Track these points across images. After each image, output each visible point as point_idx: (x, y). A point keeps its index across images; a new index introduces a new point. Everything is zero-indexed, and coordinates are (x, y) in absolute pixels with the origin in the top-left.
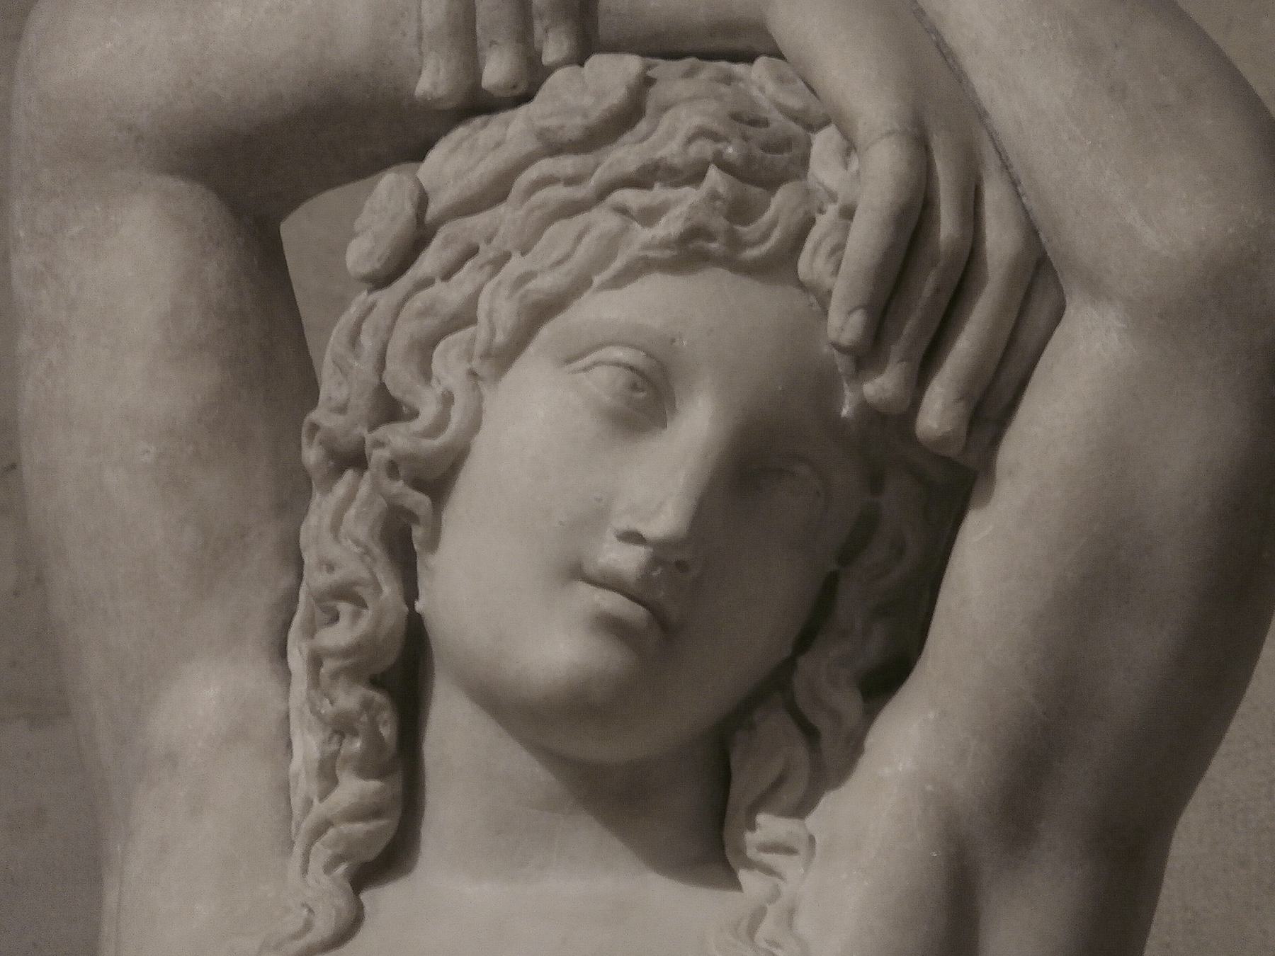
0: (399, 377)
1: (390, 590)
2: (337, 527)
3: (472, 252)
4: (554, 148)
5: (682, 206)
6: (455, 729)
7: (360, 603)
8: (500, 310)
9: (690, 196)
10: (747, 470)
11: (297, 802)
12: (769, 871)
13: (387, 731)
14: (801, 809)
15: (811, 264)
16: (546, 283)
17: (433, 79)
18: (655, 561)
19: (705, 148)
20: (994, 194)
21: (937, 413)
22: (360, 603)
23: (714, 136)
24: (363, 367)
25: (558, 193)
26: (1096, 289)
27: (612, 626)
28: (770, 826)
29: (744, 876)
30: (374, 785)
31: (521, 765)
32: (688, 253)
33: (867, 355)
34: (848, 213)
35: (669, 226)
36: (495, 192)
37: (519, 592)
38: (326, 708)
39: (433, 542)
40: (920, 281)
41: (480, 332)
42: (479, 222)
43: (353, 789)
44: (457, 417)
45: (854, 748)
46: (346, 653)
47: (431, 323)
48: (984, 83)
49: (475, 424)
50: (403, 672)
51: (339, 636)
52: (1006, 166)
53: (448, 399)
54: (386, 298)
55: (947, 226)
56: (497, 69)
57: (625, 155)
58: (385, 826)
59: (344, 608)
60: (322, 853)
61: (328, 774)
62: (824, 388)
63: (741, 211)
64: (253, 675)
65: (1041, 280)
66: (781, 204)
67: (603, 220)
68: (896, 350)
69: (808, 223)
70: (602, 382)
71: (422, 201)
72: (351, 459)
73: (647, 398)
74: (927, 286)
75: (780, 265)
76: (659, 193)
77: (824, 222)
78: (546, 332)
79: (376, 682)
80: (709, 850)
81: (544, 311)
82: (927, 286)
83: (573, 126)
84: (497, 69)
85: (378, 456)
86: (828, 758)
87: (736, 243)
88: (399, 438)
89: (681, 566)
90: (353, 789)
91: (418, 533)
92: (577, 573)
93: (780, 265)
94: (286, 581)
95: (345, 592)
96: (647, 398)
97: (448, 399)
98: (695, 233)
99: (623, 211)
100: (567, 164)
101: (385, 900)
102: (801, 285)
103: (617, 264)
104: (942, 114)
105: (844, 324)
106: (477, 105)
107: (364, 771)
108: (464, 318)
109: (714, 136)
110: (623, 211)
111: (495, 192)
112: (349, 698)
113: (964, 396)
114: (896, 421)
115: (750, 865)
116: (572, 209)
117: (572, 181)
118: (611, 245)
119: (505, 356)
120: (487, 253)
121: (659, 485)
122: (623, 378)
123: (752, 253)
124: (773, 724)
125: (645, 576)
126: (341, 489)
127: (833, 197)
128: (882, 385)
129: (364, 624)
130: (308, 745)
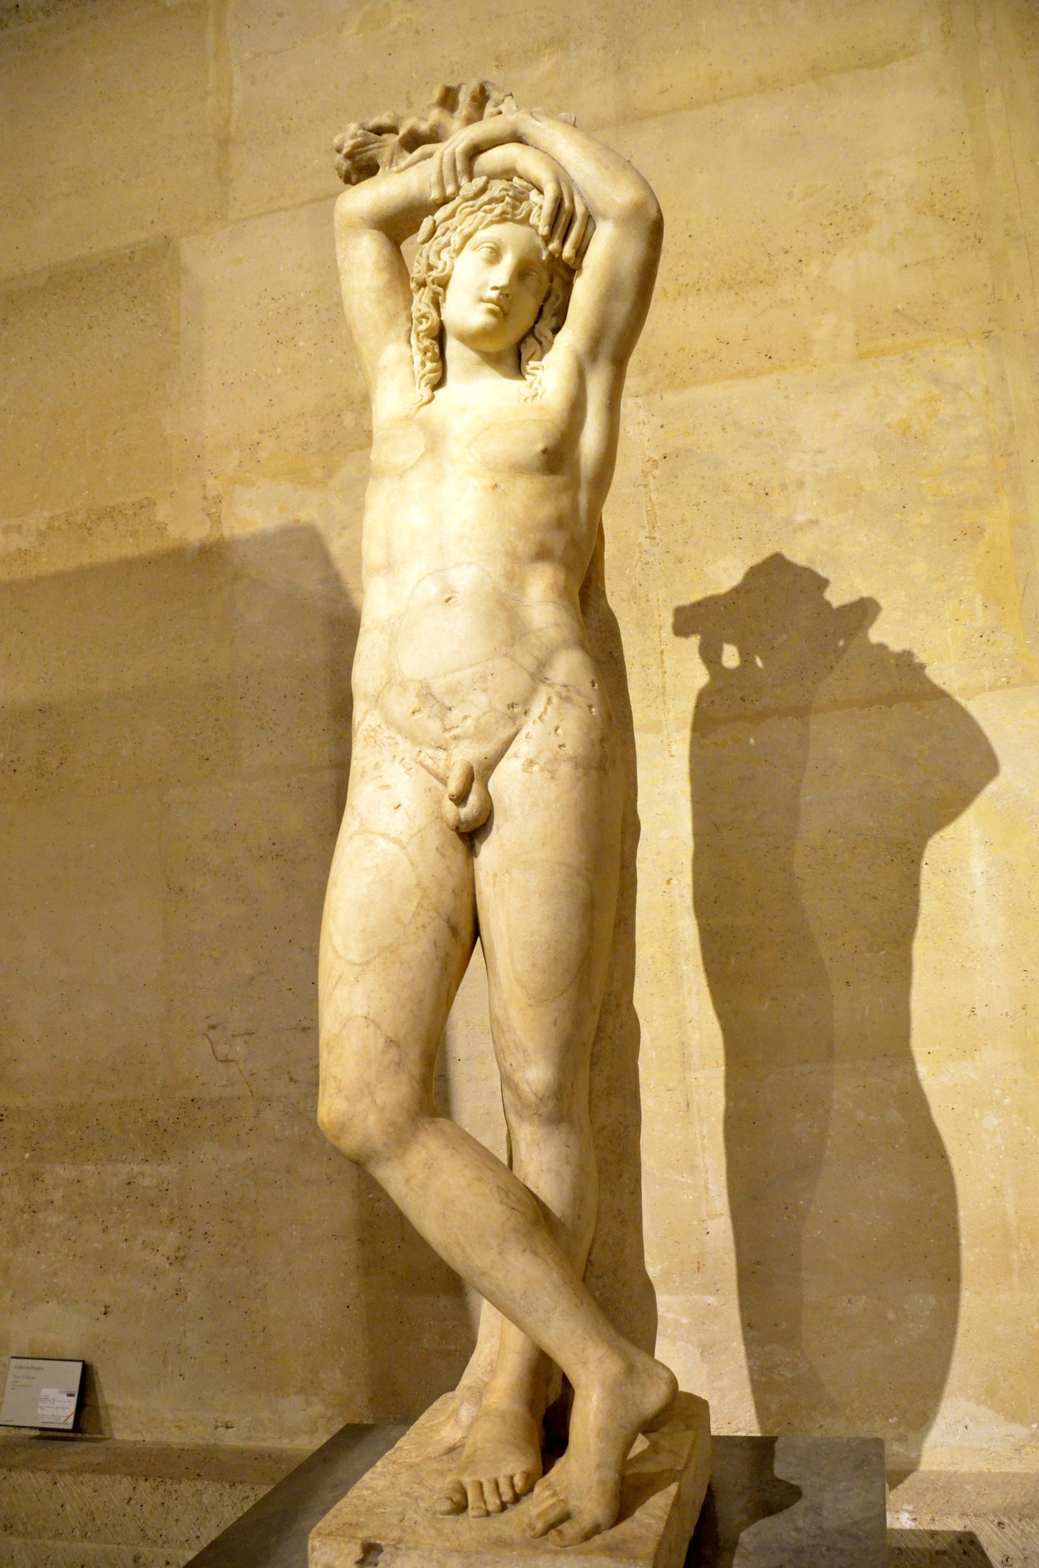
0: (433, 260)
1: (435, 314)
2: (421, 302)
3: (448, 229)
4: (467, 200)
5: (499, 208)
6: (453, 346)
7: (428, 319)
8: (456, 239)
9: (501, 205)
10: (522, 272)
11: (416, 373)
12: (533, 375)
13: (437, 350)
14: (540, 359)
15: (533, 220)
16: (468, 230)
17: (435, 194)
18: (501, 294)
19: (504, 193)
20: (577, 199)
21: (568, 252)
22: (428, 319)
23: (506, 190)
24: (423, 261)
25: (470, 209)
26: (605, 217)
27: (492, 312)
28: (532, 364)
29: (527, 376)
30: (435, 364)
31: (471, 355)
32: (503, 218)
33: (547, 240)
34: (541, 208)
35: (498, 211)
36: (452, 215)
37: (467, 309)
38: (421, 346)
39: (444, 300)
40: (561, 219)
41: (452, 248)
42: (450, 221)
43: (430, 365)
44: (448, 267)
45: (551, 344)
46: (425, 331)
47: (439, 246)
48: (572, 172)
49: (452, 269)
50: (440, 336)
51: (424, 326)
52: (579, 192)
53: (445, 264)
54: (427, 245)
55: (567, 204)
56: (450, 190)
57: (485, 198)
58: (438, 374)
59: (424, 320)
60: (423, 382)
61: (423, 364)
62: (538, 252)
63: (514, 207)
64: (403, 347)
65: (589, 219)
66: (524, 206)
67: (480, 214)
68: (556, 236)
69: (531, 211)
70: (484, 252)
71: (435, 222)
72: (423, 284)
73: (495, 255)
74: (563, 219)
75: (525, 221)
76: (493, 205)
77: (535, 209)
78: (469, 243)
79: (434, 339)
80: (518, 371)
81: (468, 237)
82: (563, 219)
83: (471, 194)
84: (450, 190)
85: (429, 280)
86: (544, 347)
87: (514, 215)
88: (434, 274)
89: (507, 296)
90: (430, 365)
91: (440, 298)
92: (481, 300)
93: (525, 221)
94: (409, 325)
95: (424, 316)
96: (495, 255)
97: (445, 264)
98: (504, 213)
99: (485, 211)
100: (470, 203)
101: (439, 393)
102: (531, 226)
103: (485, 223)
104: (561, 178)
105: (544, 230)
106: (445, 201)
107: (432, 361)
108: (448, 244)
109: (506, 190)
110: (485, 211)
111: (452, 215)
112: (427, 342)
113: (574, 247)
114: (555, 259)
115: (528, 374)
116: (472, 213)
117: (472, 206)
118: (483, 219)
119: (459, 251)
120: (452, 228)
121: (501, 274)
122: (489, 250)
123: (518, 218)
124: (531, 340)
125: (498, 299)
126: (421, 292)
127: (536, 204)
128: (554, 246)
129: (429, 323)
130: (418, 358)
